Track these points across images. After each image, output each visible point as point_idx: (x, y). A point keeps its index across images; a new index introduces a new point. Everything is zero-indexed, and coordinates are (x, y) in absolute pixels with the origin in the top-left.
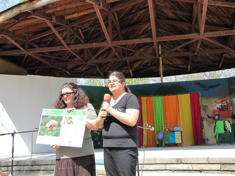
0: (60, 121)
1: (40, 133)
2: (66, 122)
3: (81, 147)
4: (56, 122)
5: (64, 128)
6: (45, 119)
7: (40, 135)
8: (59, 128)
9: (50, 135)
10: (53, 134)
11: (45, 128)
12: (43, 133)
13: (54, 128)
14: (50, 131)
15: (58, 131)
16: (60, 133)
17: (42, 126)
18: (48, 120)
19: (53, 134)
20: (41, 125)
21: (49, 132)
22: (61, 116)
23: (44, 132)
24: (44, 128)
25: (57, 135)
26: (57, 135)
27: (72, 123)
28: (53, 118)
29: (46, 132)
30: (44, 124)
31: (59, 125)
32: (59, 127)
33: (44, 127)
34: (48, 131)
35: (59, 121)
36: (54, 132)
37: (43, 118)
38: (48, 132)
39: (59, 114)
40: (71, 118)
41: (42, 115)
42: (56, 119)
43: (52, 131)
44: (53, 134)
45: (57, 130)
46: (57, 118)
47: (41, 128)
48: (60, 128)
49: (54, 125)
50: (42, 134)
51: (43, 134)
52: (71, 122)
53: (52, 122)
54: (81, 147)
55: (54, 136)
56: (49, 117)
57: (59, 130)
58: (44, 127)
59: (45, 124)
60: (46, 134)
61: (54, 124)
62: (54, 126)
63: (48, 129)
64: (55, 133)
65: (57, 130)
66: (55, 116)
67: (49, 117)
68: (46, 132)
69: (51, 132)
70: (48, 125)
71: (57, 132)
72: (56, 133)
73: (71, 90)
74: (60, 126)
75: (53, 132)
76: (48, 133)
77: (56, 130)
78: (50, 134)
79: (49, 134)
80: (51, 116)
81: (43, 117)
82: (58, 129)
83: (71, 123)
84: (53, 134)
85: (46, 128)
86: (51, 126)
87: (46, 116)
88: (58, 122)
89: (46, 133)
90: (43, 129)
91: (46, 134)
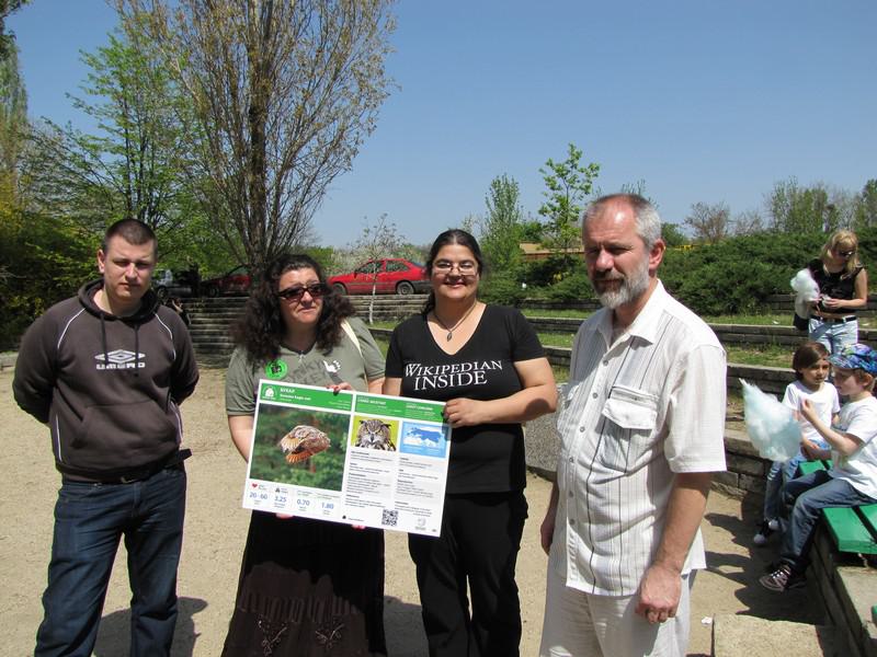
1: (257, 470)
2: (368, 438)
3: (438, 534)
4: (323, 434)
5: (357, 459)
6: (273, 419)
7: (258, 477)
8: (339, 460)
9: (302, 481)
10: (315, 480)
11: (277, 455)
12: (268, 470)
13: (315, 457)
15: (334, 470)
16: (341, 476)
17: (262, 443)
18: (285, 425)
19: (311, 477)
21: (297, 471)
23: (273, 466)
24: (271, 453)
25: (333, 482)
26: (333, 482)
27: (392, 445)
28: (308, 418)
29: (284, 468)
30: (270, 438)
31: (338, 450)
32: (337, 456)
33: (270, 451)
35: (335, 431)
36: (315, 471)
37: (265, 418)
38: (292, 470)
40: (387, 426)
41: (259, 401)
42: (321, 425)
43: (307, 468)
46: (325, 422)
47: (258, 453)
48: (344, 461)
49: (315, 444)
51: (271, 475)
52: (386, 441)
53: (303, 433)
54: (438, 534)
55: (320, 486)
56: (291, 413)
57: (342, 469)
59: (277, 440)
60: (283, 476)
61: (313, 441)
63: (290, 459)
64: (321, 476)
65: (330, 465)
68: (284, 468)
69: (304, 472)
70: (287, 444)
71: (328, 473)
72: (325, 477)
75: (311, 473)
77: (325, 466)
78: (298, 478)
79: (295, 475)
80: (297, 410)
82: (334, 461)
83: (386, 446)
85: (280, 451)
86: (299, 450)
90: (267, 457)
91: (283, 476)
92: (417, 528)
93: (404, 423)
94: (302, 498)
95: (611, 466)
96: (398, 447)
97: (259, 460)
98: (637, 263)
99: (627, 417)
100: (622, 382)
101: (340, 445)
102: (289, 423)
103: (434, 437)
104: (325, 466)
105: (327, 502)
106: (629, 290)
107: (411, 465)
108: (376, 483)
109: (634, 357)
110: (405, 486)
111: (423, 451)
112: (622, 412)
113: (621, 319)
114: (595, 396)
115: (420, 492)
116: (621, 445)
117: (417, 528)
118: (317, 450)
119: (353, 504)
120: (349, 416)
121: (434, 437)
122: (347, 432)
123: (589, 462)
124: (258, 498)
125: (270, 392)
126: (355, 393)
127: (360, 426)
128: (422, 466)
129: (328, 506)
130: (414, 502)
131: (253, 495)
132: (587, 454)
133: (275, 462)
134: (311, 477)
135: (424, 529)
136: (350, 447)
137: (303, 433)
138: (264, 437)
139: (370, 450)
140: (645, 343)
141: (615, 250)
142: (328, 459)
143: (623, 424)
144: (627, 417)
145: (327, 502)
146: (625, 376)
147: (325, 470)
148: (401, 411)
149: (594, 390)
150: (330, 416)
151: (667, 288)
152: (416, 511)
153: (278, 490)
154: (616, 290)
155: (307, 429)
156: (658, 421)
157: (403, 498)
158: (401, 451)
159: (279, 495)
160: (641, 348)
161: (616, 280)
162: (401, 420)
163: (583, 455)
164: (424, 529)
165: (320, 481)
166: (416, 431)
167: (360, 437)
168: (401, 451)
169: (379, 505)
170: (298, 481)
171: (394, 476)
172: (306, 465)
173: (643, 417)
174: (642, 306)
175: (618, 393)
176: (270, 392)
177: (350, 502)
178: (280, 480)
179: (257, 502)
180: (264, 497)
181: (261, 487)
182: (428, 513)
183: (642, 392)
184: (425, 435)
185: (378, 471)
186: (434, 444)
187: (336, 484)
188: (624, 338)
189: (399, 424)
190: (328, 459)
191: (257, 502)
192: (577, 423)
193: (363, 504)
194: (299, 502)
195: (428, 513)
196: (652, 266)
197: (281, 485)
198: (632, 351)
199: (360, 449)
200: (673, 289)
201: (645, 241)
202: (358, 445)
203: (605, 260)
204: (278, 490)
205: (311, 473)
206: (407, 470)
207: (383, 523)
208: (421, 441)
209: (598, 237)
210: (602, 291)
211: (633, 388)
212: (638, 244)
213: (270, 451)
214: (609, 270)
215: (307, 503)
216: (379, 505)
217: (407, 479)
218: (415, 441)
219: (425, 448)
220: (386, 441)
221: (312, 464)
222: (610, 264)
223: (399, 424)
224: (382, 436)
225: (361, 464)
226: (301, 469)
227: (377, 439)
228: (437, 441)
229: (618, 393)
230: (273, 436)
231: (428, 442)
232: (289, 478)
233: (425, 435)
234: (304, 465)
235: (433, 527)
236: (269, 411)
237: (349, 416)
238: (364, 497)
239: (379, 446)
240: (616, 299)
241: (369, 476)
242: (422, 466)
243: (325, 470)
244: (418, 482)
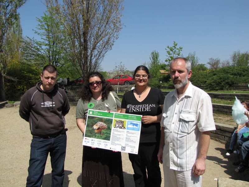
0: (110, 125)
2: (118, 125)
3: (137, 153)
5: (115, 131)
6: (92, 120)
7: (87, 136)
8: (109, 132)
9: (99, 138)
10: (103, 137)
11: (92, 130)
12: (90, 134)
13: (103, 131)
14: (98, 134)
16: (110, 136)
17: (88, 127)
18: (94, 122)
21: (98, 135)
22: (111, 119)
23: (91, 133)
24: (91, 130)
25: (107, 138)
26: (107, 138)
27: (124, 127)
28: (101, 120)
29: (94, 134)
30: (91, 125)
31: (109, 129)
32: (109, 130)
33: (91, 129)
35: (109, 123)
36: (103, 135)
37: (90, 120)
38: (96, 135)
40: (123, 122)
43: (101, 134)
44: (101, 137)
45: (107, 133)
47: (87, 130)
48: (111, 132)
50: (89, 136)
51: (90, 136)
52: (123, 126)
53: (100, 124)
54: (137, 153)
56: (97, 118)
57: (110, 134)
58: (91, 128)
59: (92, 126)
60: (94, 136)
61: (102, 126)
63: (96, 131)
64: (104, 136)
65: (107, 133)
66: (103, 118)
68: (94, 134)
69: (99, 135)
70: (95, 127)
71: (106, 135)
72: (105, 136)
73: (100, 79)
74: (111, 130)
75: (101, 135)
76: (95, 135)
77: (106, 133)
78: (98, 137)
80: (98, 117)
82: (108, 132)
83: (123, 128)
86: (99, 129)
87: (93, 117)
88: (107, 125)
89: (94, 135)
90: (90, 131)
91: (94, 136)
92: (131, 152)
93: (128, 121)
94: (99, 142)
95: (184, 132)
96: (126, 128)
97: (87, 131)
98: (184, 77)
101: (110, 127)
102: (96, 121)
103: (136, 125)
104: (106, 133)
105: (106, 144)
106: (183, 84)
108: (120, 138)
109: (187, 101)
110: (128, 139)
111: (133, 129)
113: (180, 92)
114: (176, 114)
117: (131, 152)
118: (103, 129)
119: (113, 144)
120: (113, 119)
121: (136, 125)
122: (112, 124)
123: (177, 132)
124: (87, 142)
125: (91, 113)
126: (114, 113)
127: (116, 122)
128: (133, 133)
129: (106, 145)
130: (130, 144)
131: (85, 141)
132: (176, 130)
133: (92, 132)
134: (101, 137)
135: (133, 152)
136: (113, 128)
137: (100, 124)
138: (89, 125)
139: (118, 129)
140: (189, 97)
141: (180, 72)
142: (106, 131)
145: (106, 144)
146: (185, 107)
147: (106, 135)
148: (127, 118)
150: (107, 119)
151: (193, 84)
152: (131, 146)
153: (92, 140)
154: (179, 84)
157: (127, 143)
158: (127, 129)
159: (92, 141)
160: (188, 98)
161: (179, 81)
162: (127, 120)
163: (175, 130)
164: (133, 152)
165: (104, 138)
166: (131, 123)
167: (115, 125)
168: (127, 129)
169: (120, 145)
170: (98, 138)
171: (125, 136)
172: (100, 133)
174: (187, 87)
175: (184, 112)
176: (91, 113)
177: (113, 144)
178: (93, 137)
179: (86, 144)
180: (88, 142)
182: (134, 147)
184: (134, 124)
186: (136, 127)
187: (108, 139)
188: (183, 96)
189: (126, 121)
190: (106, 131)
191: (86, 144)
192: (171, 122)
193: (116, 145)
194: (98, 144)
195: (134, 147)
196: (189, 77)
197: (93, 139)
198: (186, 99)
199: (115, 129)
200: (196, 84)
201: (188, 70)
202: (115, 128)
203: (177, 74)
204: (92, 140)
206: (129, 135)
207: (121, 150)
208: (133, 126)
209: (175, 68)
210: (176, 84)
212: (186, 71)
213: (91, 129)
214: (178, 77)
215: (100, 144)
216: (120, 145)
217: (129, 137)
218: (131, 126)
220: (123, 126)
221: (102, 133)
222: (178, 76)
223: (126, 121)
224: (122, 125)
225: (115, 133)
226: (98, 134)
227: (120, 126)
228: (137, 126)
229: (184, 112)
230: (91, 125)
231: (134, 126)
232: (95, 137)
233: (134, 124)
234: (100, 133)
235: (136, 151)
236: (91, 118)
237: (113, 119)
238: (116, 142)
239: (121, 128)
240: (179, 86)
241: (118, 136)
242: (133, 133)
243: (106, 135)
244: (131, 138)
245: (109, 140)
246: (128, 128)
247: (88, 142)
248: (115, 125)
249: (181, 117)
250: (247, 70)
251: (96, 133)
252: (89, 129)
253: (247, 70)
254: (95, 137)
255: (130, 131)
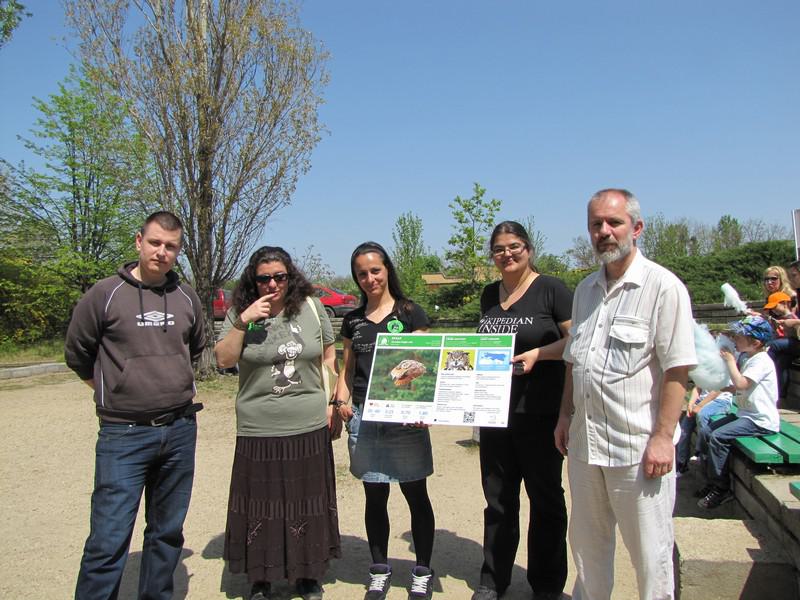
3: (505, 425)
5: (445, 378)
6: (386, 358)
7: (374, 398)
12: (382, 392)
13: (415, 380)
16: (434, 392)
19: (412, 394)
20: (373, 374)
21: (402, 391)
23: (385, 390)
25: (428, 396)
26: (428, 396)
28: (410, 355)
31: (432, 374)
32: (431, 378)
33: (384, 379)
34: (397, 388)
35: (429, 362)
37: (380, 357)
39: (430, 346)
47: (374, 382)
52: (466, 364)
53: (407, 365)
54: (505, 425)
55: (418, 400)
56: (399, 353)
57: (434, 386)
59: (388, 371)
60: (392, 396)
62: (416, 375)
63: (397, 383)
65: (426, 385)
67: (399, 353)
69: (407, 391)
70: (395, 373)
75: (412, 392)
77: (422, 385)
78: (403, 396)
81: (379, 352)
82: (429, 382)
83: (466, 367)
84: (415, 396)
85: (391, 380)
86: (404, 376)
87: (390, 352)
89: (392, 393)
90: (381, 384)
94: (405, 410)
96: (475, 367)
99: (628, 335)
100: (621, 313)
103: (501, 357)
105: (423, 410)
107: (483, 378)
108: (459, 393)
110: (480, 393)
111: (493, 368)
112: (623, 332)
114: (600, 326)
115: (493, 397)
116: (624, 355)
118: (416, 375)
119: (442, 410)
121: (501, 357)
127: (448, 356)
128: (492, 378)
130: (486, 403)
131: (370, 411)
133: (386, 386)
138: (379, 370)
139: (455, 371)
143: (626, 340)
144: (628, 335)
145: (423, 410)
148: (477, 343)
149: (599, 322)
153: (388, 406)
155: (409, 362)
156: (650, 337)
157: (479, 402)
162: (477, 349)
166: (488, 355)
167: (447, 363)
169: (461, 409)
170: (403, 398)
171: (472, 387)
172: (409, 386)
173: (638, 334)
175: (619, 321)
177: (439, 409)
178: (389, 398)
180: (377, 411)
181: (377, 405)
183: (637, 318)
184: (494, 357)
185: (459, 385)
186: (501, 362)
187: (429, 397)
189: (476, 353)
193: (449, 410)
194: (402, 412)
197: (390, 402)
204: (388, 406)
205: (412, 392)
206: (481, 382)
211: (630, 316)
215: (408, 412)
218: (488, 361)
219: (495, 366)
220: (466, 364)
221: (412, 385)
223: (476, 353)
224: (464, 362)
225: (447, 381)
227: (459, 364)
229: (619, 321)
231: (497, 361)
233: (494, 357)
235: (501, 420)
238: (451, 404)
241: (454, 389)
242: (492, 378)
244: (490, 390)
245: (432, 400)
246: (479, 368)
247: (377, 411)
248: (447, 363)
249: (612, 334)
250: (693, 267)
251: (397, 388)
252: (380, 380)
253: (693, 267)
254: (396, 396)
255: (485, 373)
